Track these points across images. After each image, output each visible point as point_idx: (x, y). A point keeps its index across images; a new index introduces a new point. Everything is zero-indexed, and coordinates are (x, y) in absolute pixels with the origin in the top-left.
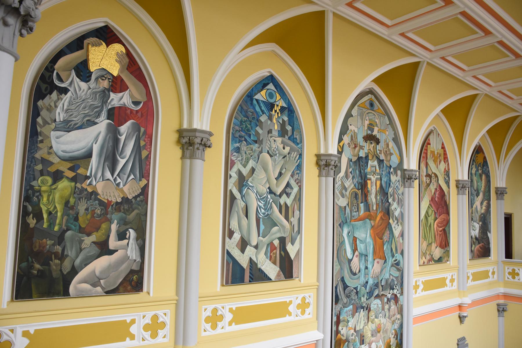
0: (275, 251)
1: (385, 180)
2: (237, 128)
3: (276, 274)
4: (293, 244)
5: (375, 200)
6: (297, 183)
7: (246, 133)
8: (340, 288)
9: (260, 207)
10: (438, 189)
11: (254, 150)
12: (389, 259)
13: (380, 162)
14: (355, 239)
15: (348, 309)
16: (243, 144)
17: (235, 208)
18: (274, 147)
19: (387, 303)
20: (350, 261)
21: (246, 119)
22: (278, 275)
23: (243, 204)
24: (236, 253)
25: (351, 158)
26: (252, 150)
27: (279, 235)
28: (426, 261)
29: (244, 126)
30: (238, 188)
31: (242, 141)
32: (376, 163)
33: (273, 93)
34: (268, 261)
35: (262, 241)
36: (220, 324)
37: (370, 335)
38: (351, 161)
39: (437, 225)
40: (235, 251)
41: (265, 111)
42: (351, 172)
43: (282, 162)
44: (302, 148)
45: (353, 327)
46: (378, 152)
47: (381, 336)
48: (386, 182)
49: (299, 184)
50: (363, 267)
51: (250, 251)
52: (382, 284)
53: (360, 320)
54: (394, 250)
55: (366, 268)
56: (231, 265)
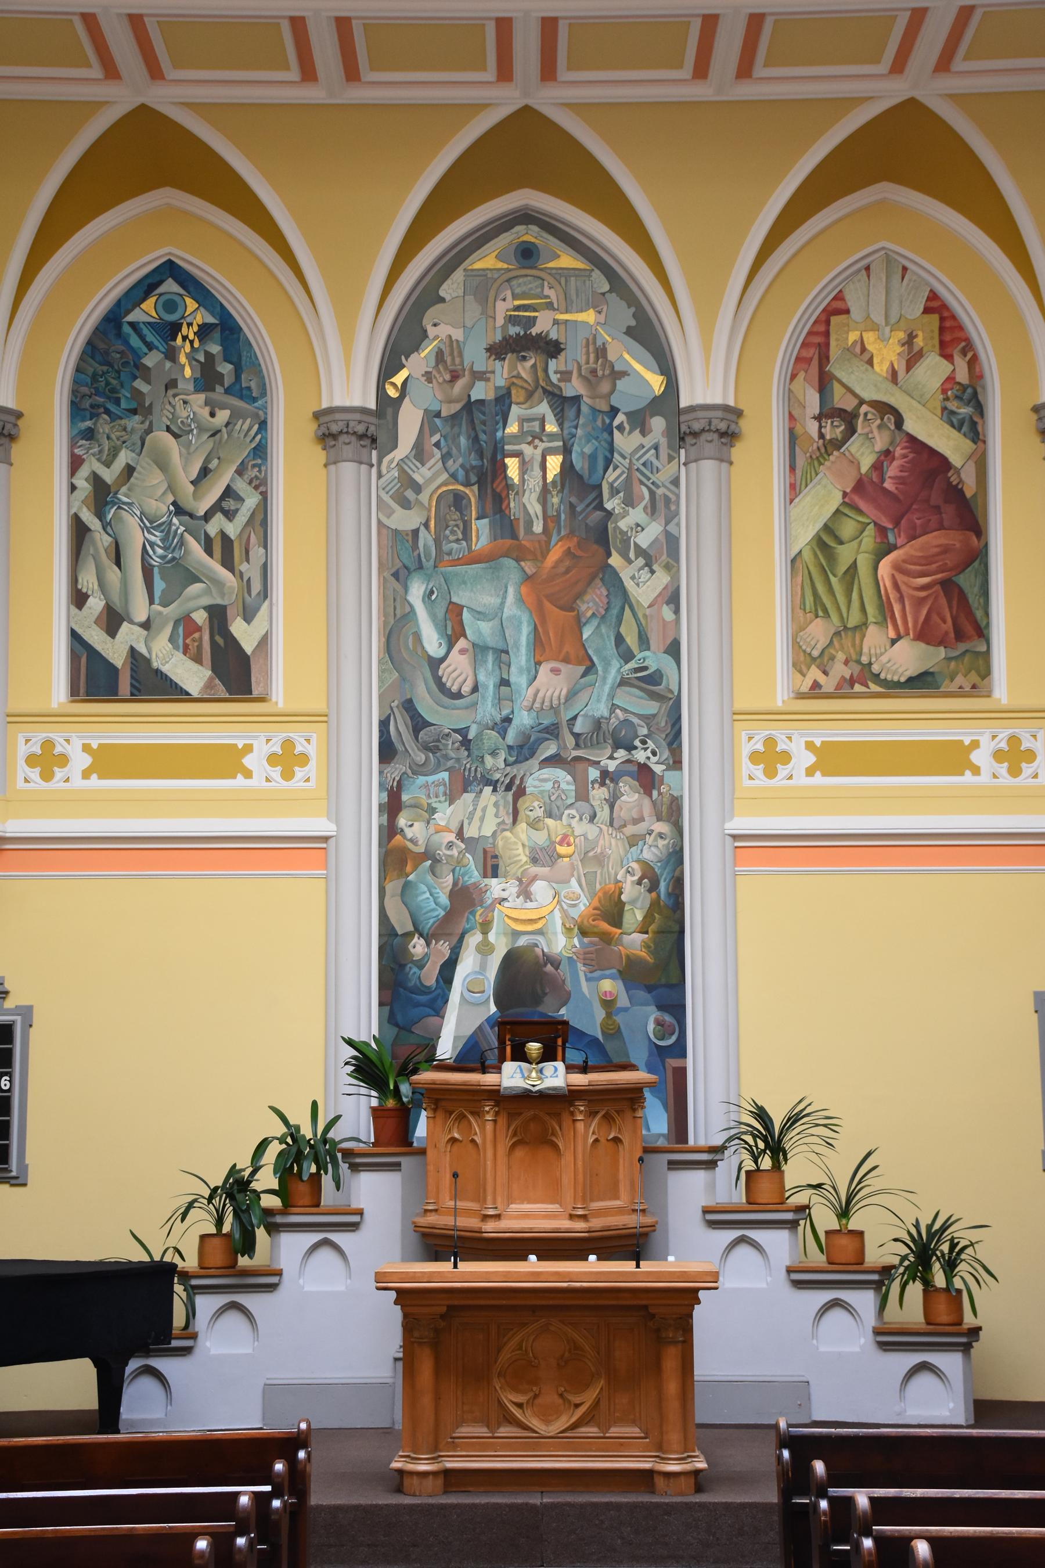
0: (196, 635)
1: (588, 450)
2: (85, 390)
3: (201, 684)
4: (248, 618)
5: (538, 508)
6: (256, 488)
7: (109, 398)
8: (400, 726)
9: (152, 545)
10: (898, 452)
11: (129, 429)
12: (607, 664)
13: (564, 405)
14: (455, 611)
15: (431, 779)
16: (101, 421)
17: (88, 549)
18: (184, 414)
19: (603, 784)
20: (435, 663)
21: (105, 368)
22: (209, 686)
23: (107, 540)
24: (96, 637)
25: (435, 407)
26: (125, 429)
27: (207, 601)
28: (828, 684)
29: (103, 384)
30: (93, 510)
31: (98, 415)
32: (544, 408)
33: (177, 298)
34: (179, 655)
35: (160, 613)
36: (59, 773)
37: (524, 859)
38: (438, 415)
39: (897, 567)
40: (94, 633)
41: (156, 343)
42: (437, 445)
43: (210, 445)
44: (264, 408)
45: (454, 826)
46: (554, 378)
47: (573, 867)
48: (592, 458)
49: (262, 489)
50: (488, 680)
51: (129, 634)
52: (577, 729)
53: (479, 813)
54: (631, 640)
55: (505, 683)
56: (84, 660)
